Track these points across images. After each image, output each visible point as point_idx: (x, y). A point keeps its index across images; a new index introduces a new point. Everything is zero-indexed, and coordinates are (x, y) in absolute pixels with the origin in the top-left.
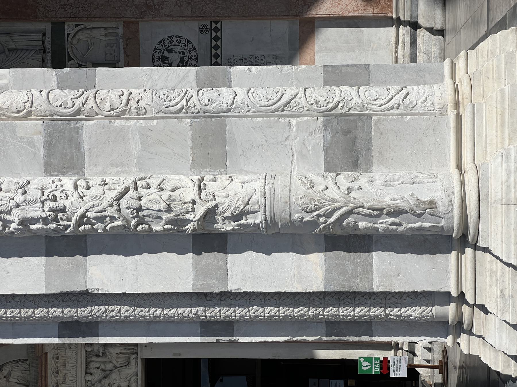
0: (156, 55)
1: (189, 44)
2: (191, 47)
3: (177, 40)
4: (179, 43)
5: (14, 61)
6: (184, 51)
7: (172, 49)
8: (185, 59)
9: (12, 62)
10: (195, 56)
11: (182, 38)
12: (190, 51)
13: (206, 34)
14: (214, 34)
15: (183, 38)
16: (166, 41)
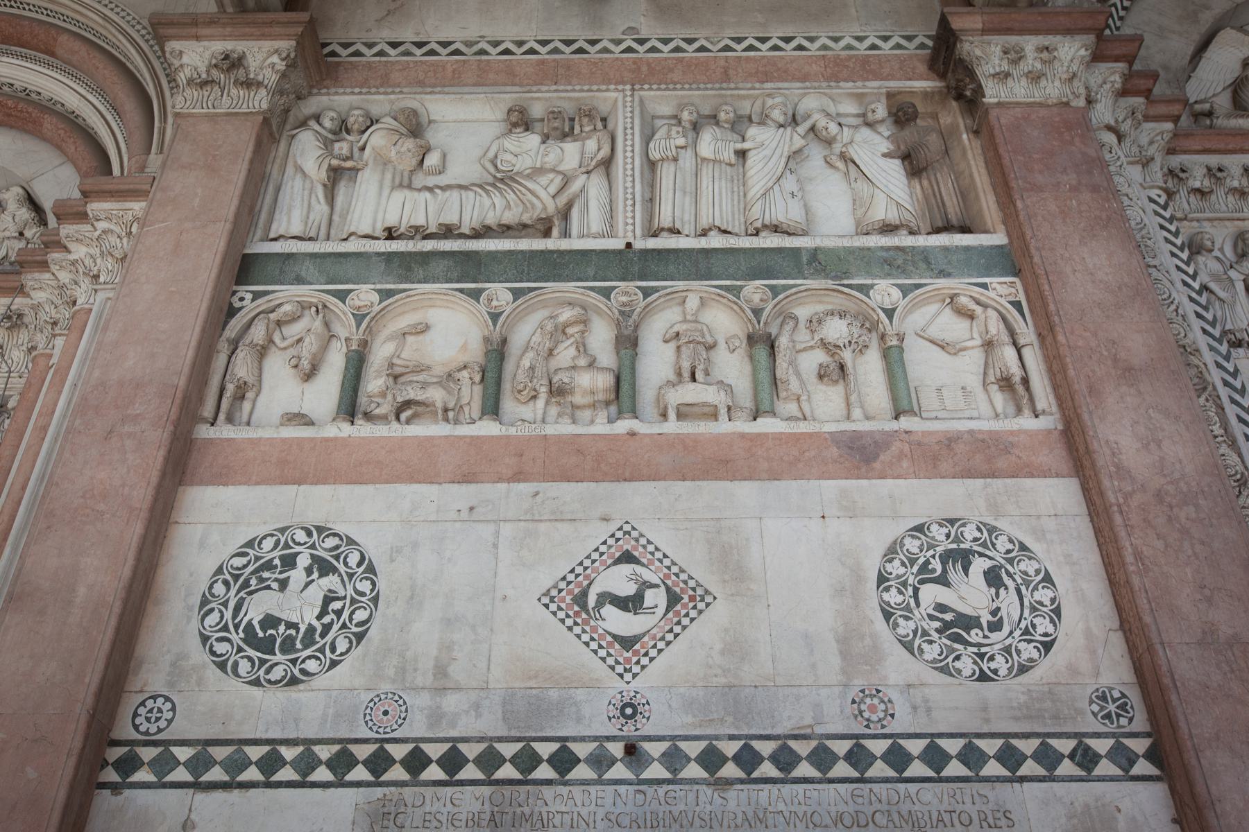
0: (970, 532)
1: (1035, 647)
2: (1025, 656)
3: (1041, 603)
4: (1033, 609)
5: (875, 166)
6: (1006, 629)
7: (1005, 585)
8: (973, 632)
9: (871, 163)
10: (995, 672)
11: (1052, 621)
12: (1007, 650)
13: (1095, 715)
14: (1102, 746)
15: (1055, 625)
16: (1029, 566)
